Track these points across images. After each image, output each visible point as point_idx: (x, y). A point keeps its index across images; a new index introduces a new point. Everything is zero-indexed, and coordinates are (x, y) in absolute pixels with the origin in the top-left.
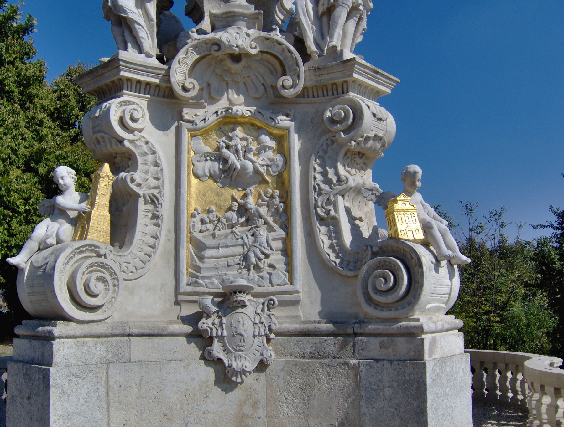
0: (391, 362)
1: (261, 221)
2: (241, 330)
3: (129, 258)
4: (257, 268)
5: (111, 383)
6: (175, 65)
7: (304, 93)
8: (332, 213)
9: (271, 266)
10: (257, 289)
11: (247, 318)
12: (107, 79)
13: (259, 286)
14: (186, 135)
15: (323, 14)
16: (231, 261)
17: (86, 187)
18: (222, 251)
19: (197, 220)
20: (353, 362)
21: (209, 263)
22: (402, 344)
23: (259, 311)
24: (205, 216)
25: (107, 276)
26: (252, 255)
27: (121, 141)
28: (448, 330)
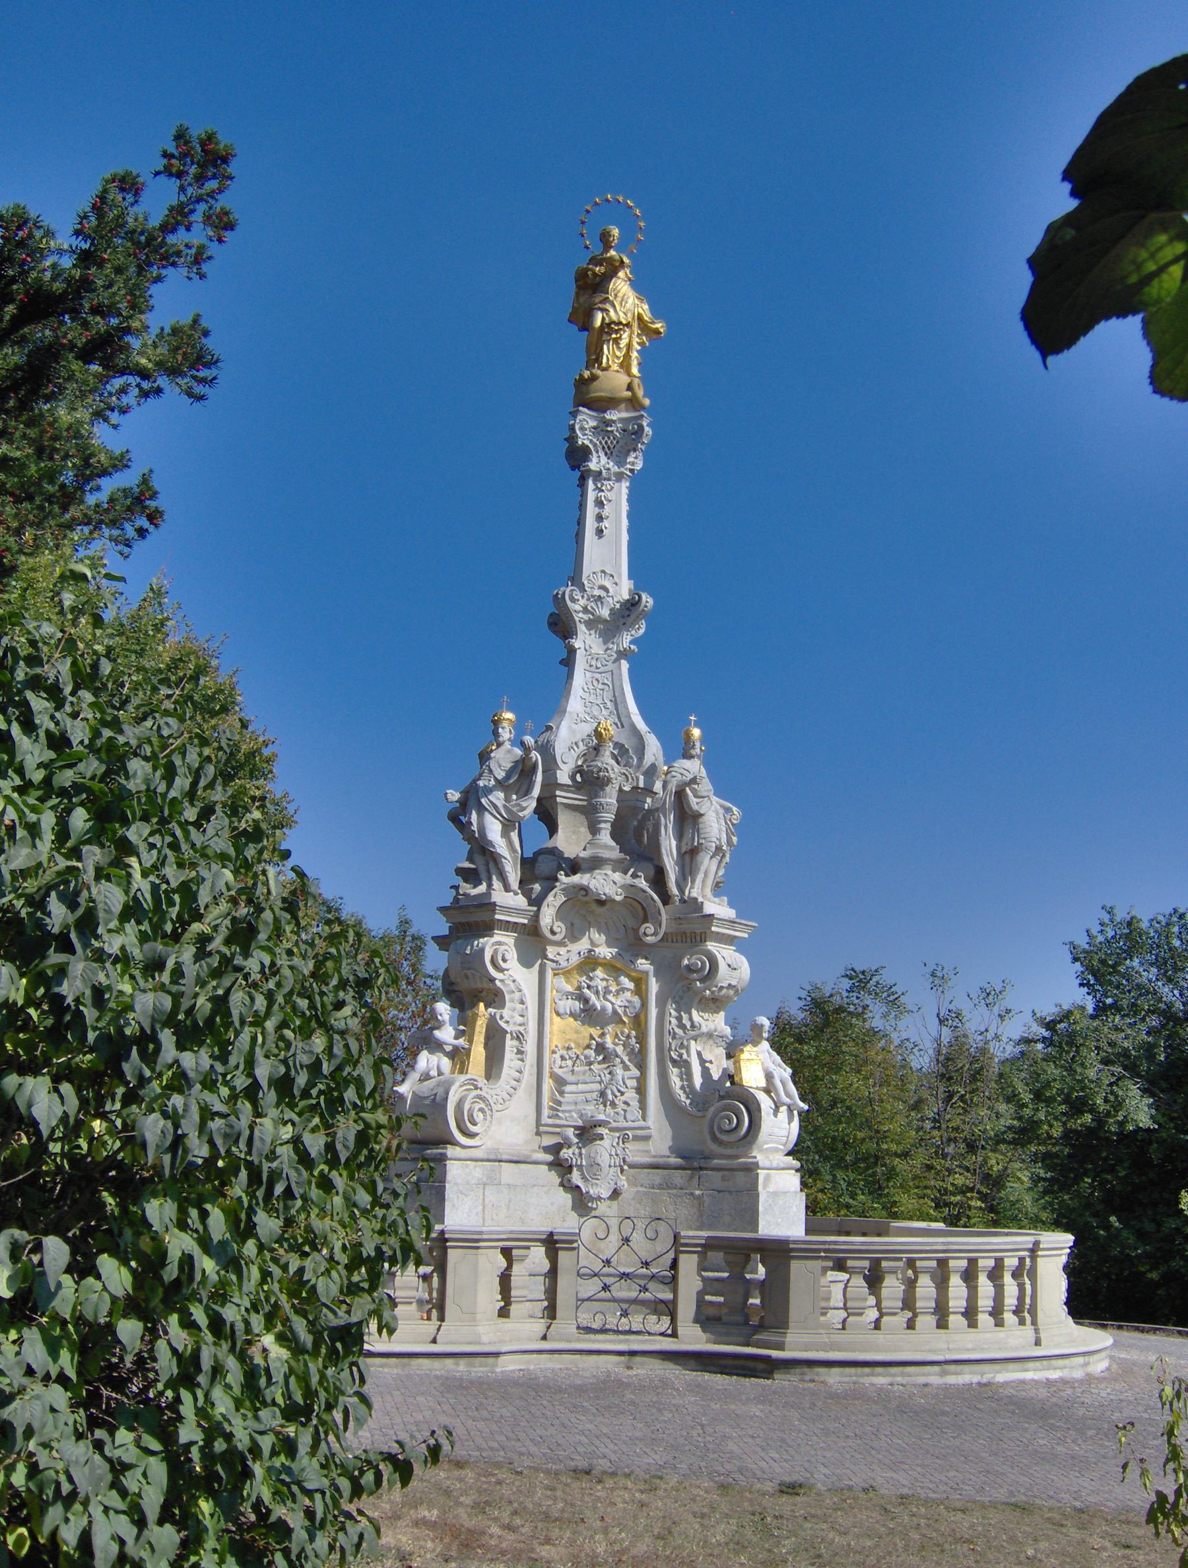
0: (730, 1192)
2: (599, 1160)
3: (498, 1091)
4: (613, 1104)
5: (487, 1201)
6: (544, 908)
8: (685, 1056)
9: (626, 1103)
10: (614, 1125)
11: (605, 1149)
14: (549, 974)
16: (589, 1096)
18: (581, 1087)
19: (557, 1056)
20: (697, 1192)
21: (568, 1097)
22: (740, 1177)
24: (564, 1052)
25: (483, 1105)
26: (609, 1092)
27: (493, 980)
28: (783, 1169)
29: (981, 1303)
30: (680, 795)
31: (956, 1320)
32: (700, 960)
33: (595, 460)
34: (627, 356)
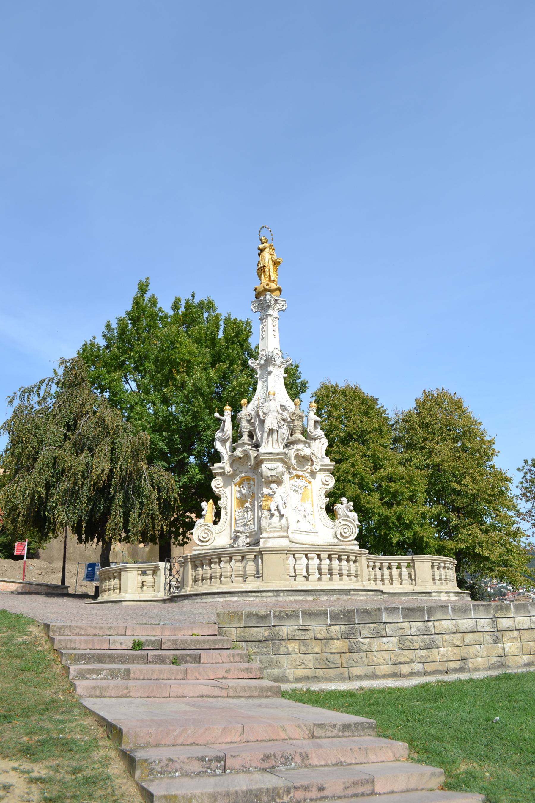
21: (238, 525)
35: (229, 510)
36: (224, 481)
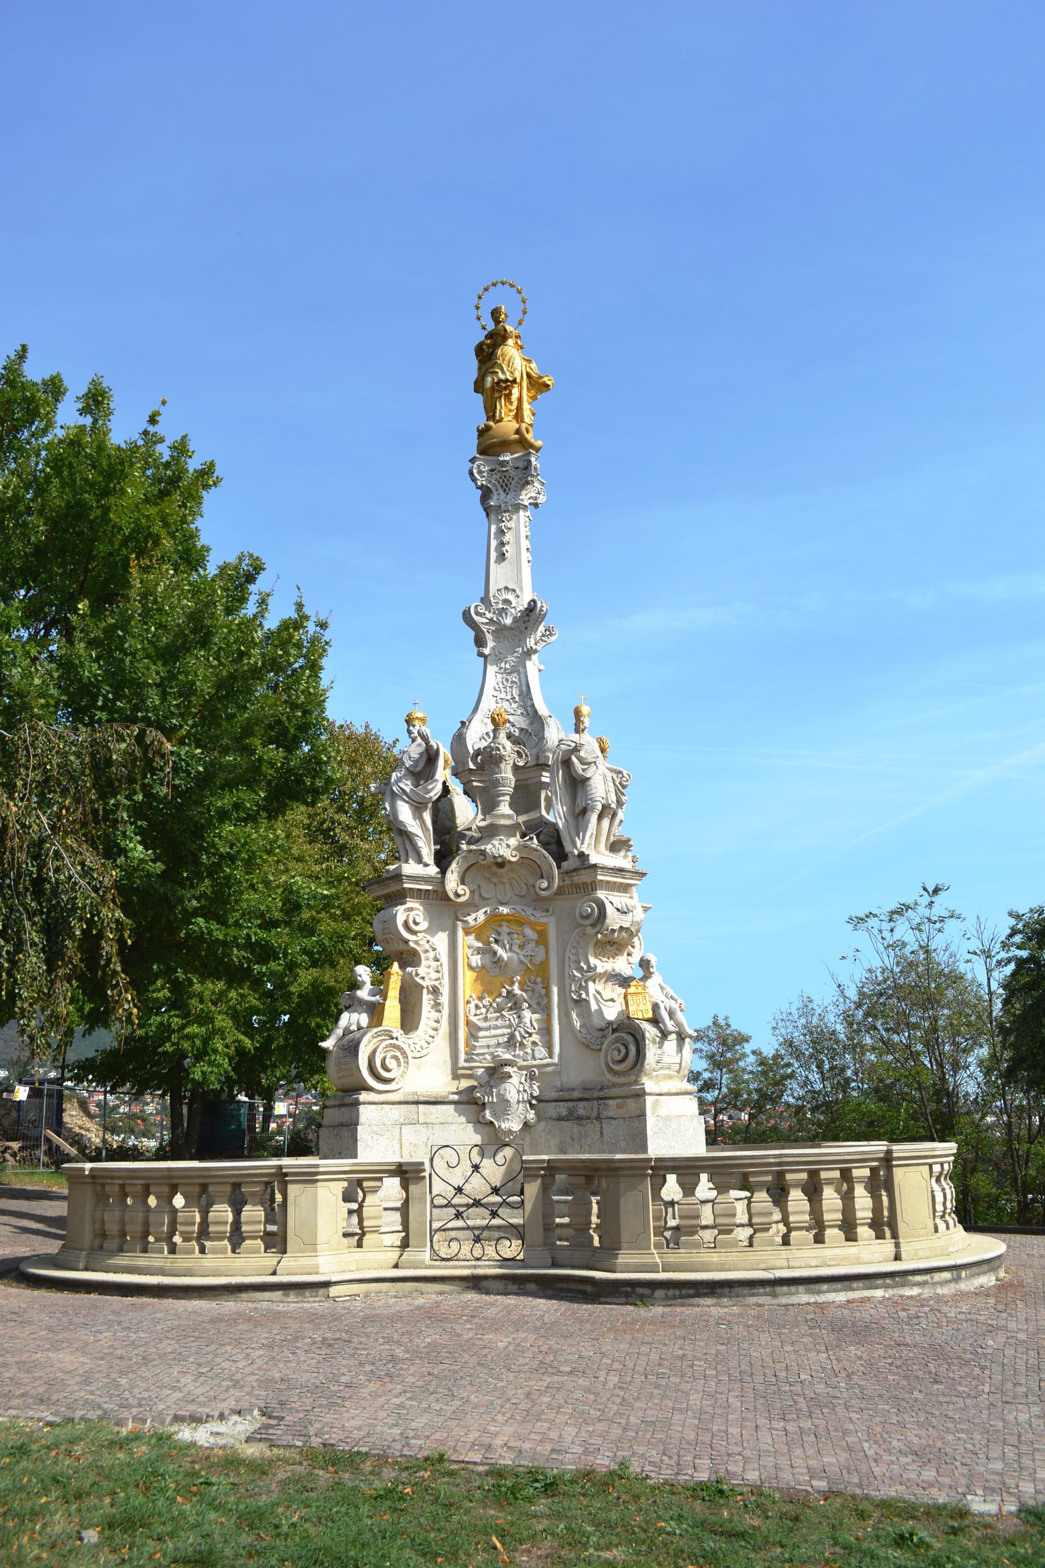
0: (624, 1119)
1: (526, 1005)
2: (508, 1097)
3: (416, 1040)
4: (522, 1044)
6: (449, 875)
7: (560, 892)
8: (584, 996)
10: (521, 1063)
12: (394, 888)
13: (524, 1060)
14: (460, 933)
15: (579, 814)
17: (380, 984)
18: (493, 1032)
19: (472, 1005)
21: (482, 1042)
22: (631, 1103)
23: (523, 1081)
25: (398, 1054)
27: (407, 942)
28: (677, 1094)
29: (859, 1214)
30: (567, 763)
31: (833, 1234)
32: (590, 907)
33: (495, 497)
34: (519, 408)
35: (445, 999)
36: (430, 915)
